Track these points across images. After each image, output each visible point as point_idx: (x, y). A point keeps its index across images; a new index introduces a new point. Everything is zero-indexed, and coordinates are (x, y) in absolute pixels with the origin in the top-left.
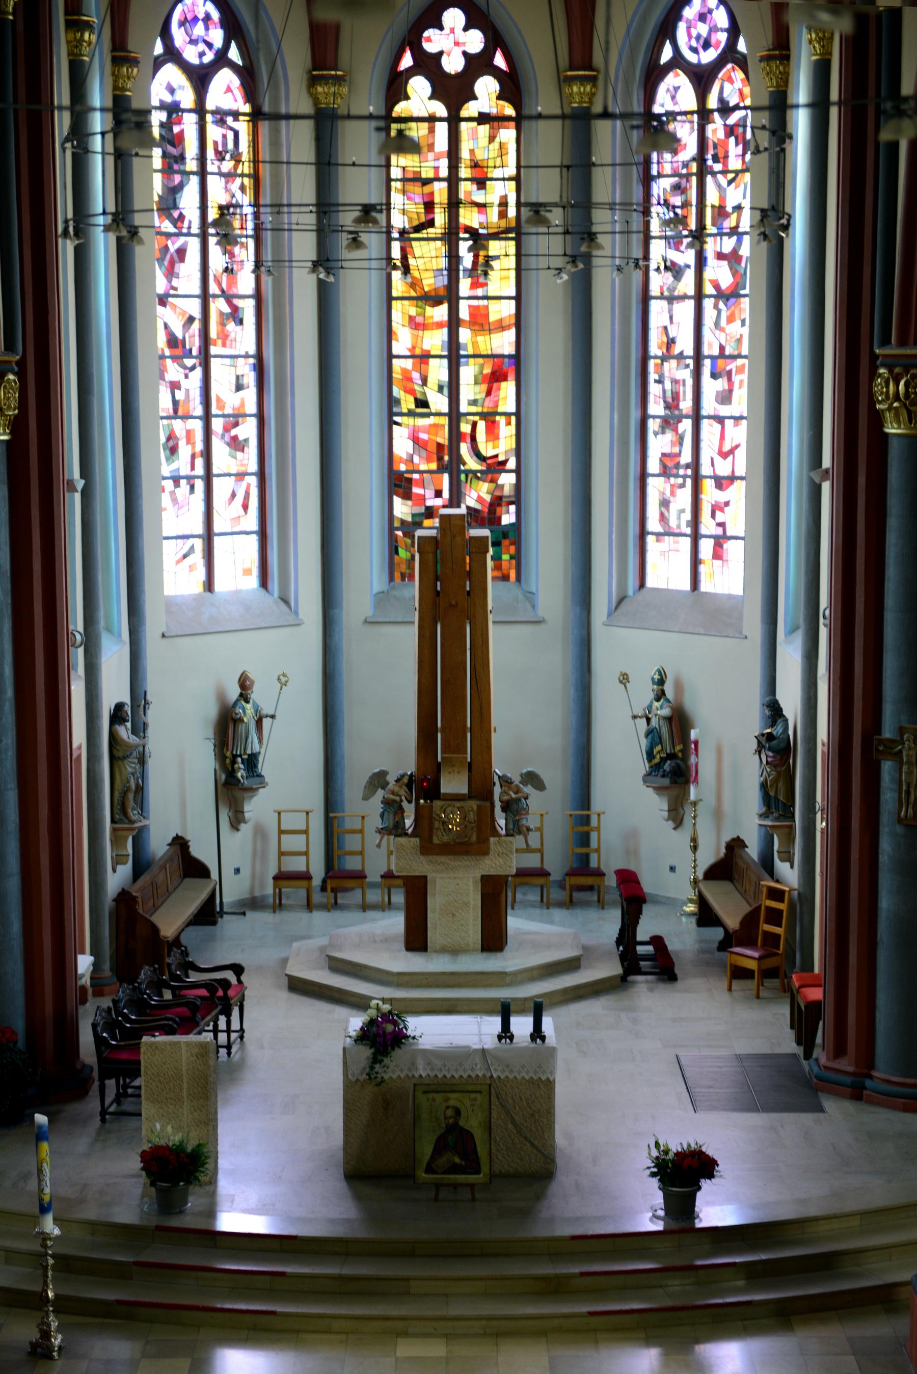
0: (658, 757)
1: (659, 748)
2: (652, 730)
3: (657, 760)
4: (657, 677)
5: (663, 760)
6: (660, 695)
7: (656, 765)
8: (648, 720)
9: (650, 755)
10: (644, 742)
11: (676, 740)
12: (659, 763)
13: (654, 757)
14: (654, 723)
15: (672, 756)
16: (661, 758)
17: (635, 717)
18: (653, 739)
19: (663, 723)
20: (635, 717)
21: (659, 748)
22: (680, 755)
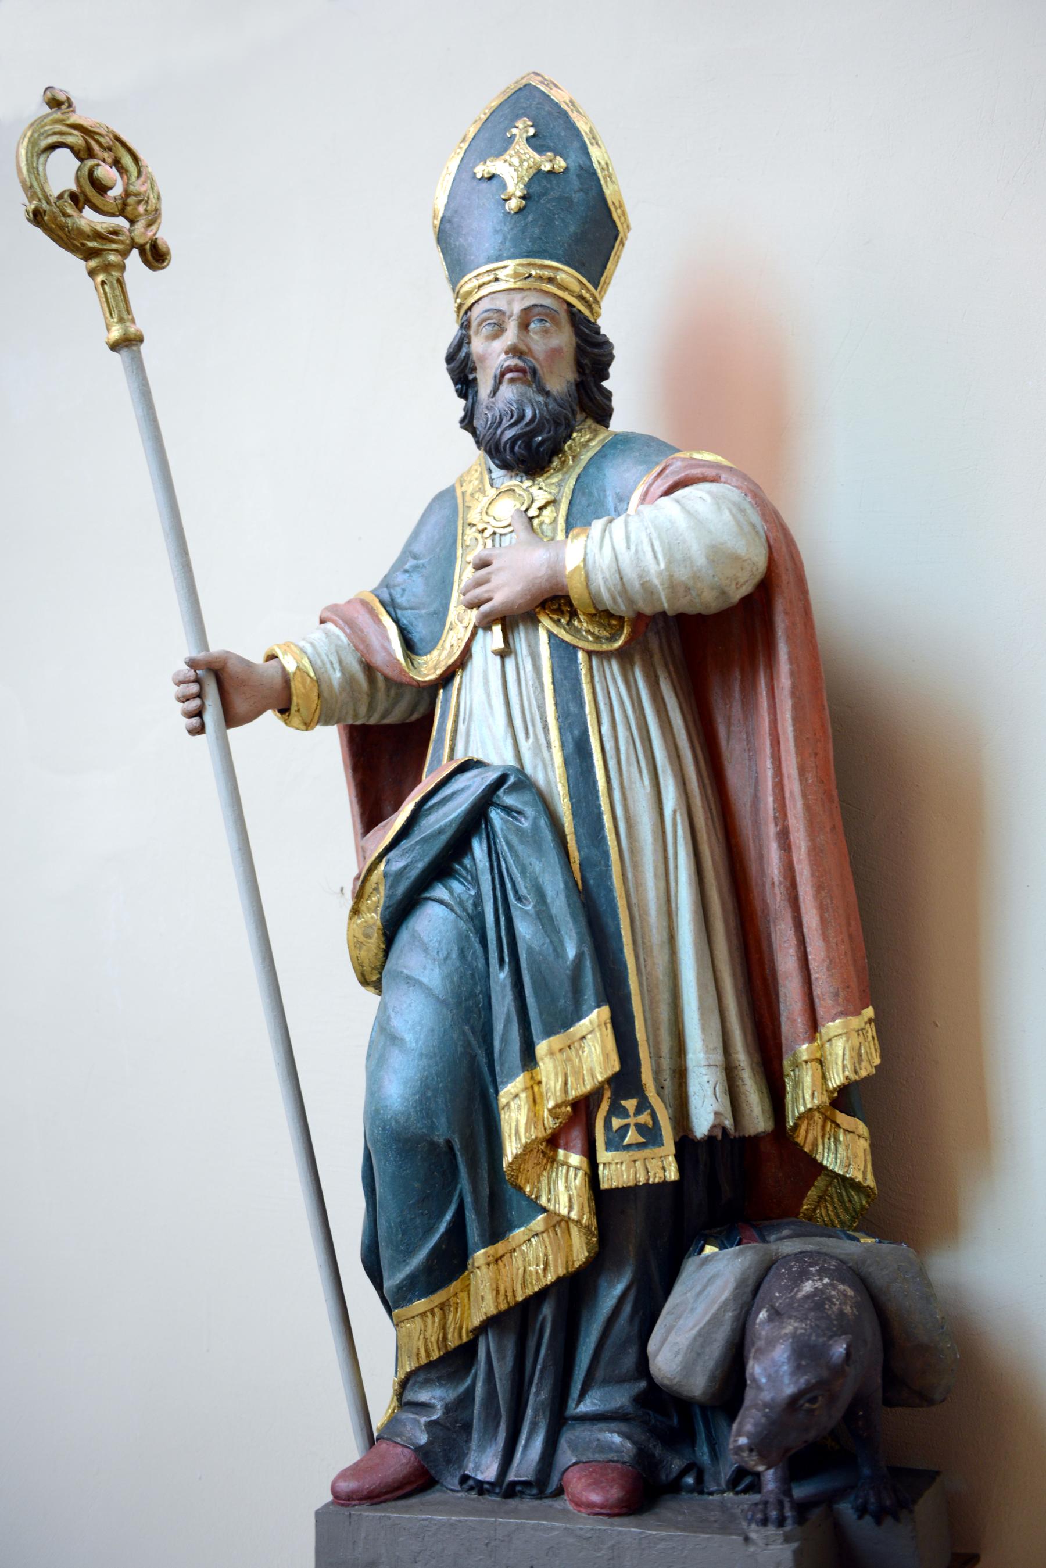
0: (564, 1191)
1: (583, 1054)
2: (476, 820)
3: (533, 1257)
4: (514, 168)
5: (636, 1244)
6: (549, 415)
7: (516, 1319)
8: (388, 744)
9: (439, 1181)
10: (356, 1050)
11: (807, 944)
12: (573, 1291)
13: (501, 1208)
14: (494, 717)
15: (743, 1181)
16: (604, 1201)
17: (224, 692)
18: (490, 937)
19: (626, 710)
20: (224, 692)
21: (583, 1054)
22: (845, 1153)
